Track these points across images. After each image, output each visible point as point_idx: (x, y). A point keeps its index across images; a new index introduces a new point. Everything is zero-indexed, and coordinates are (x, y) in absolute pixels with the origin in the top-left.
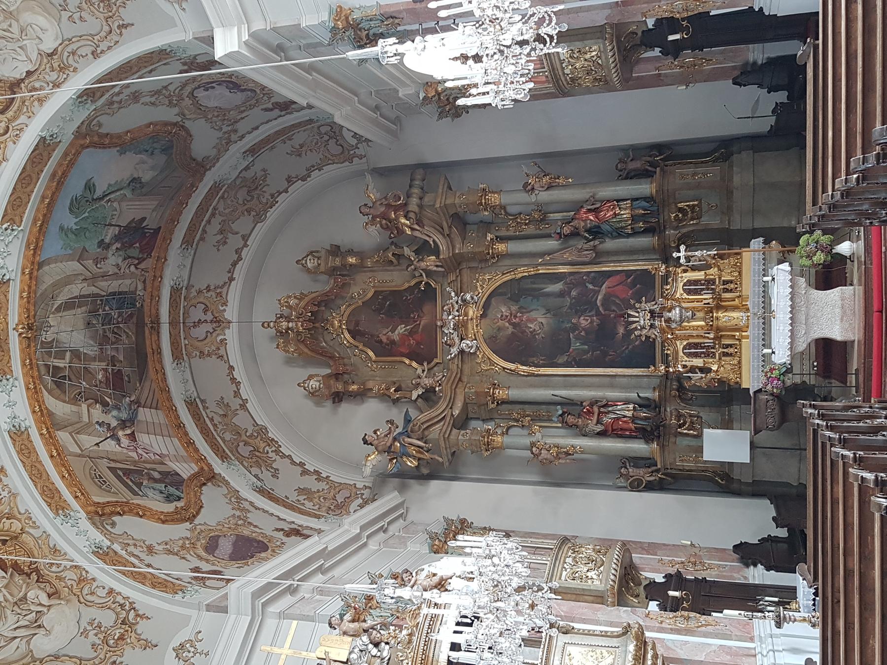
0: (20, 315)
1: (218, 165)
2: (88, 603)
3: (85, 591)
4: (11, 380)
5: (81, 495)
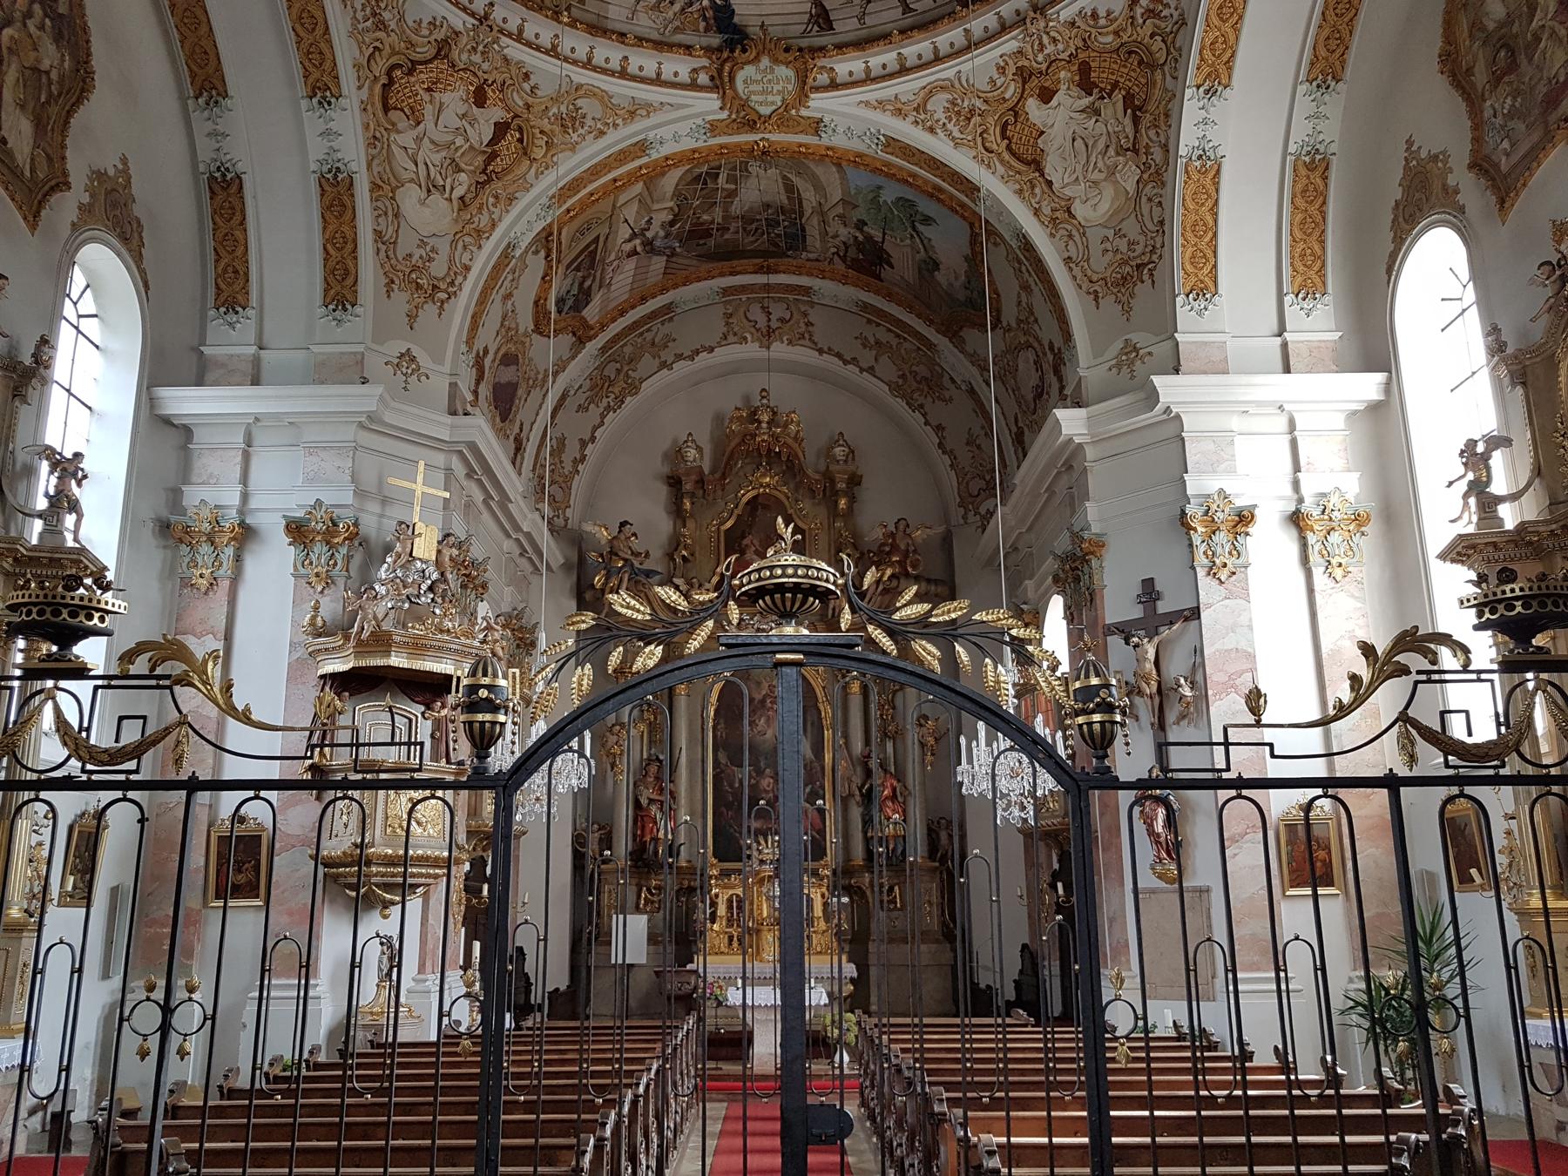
0: (779, 143)
1: (956, 350)
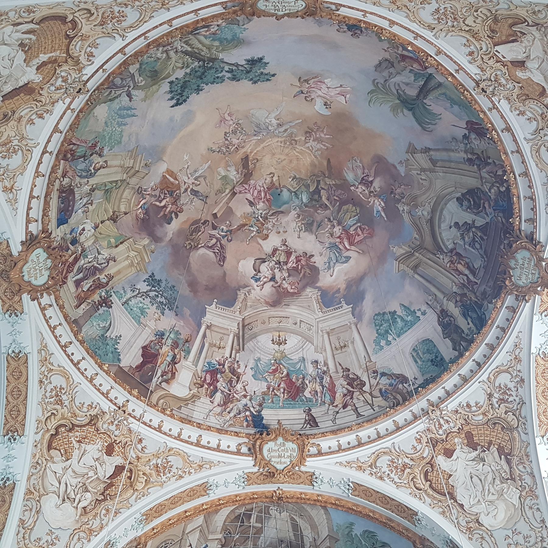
0: (289, 492)
2: (73, 535)
3: (82, 534)
4: (243, 484)
5: (155, 533)
